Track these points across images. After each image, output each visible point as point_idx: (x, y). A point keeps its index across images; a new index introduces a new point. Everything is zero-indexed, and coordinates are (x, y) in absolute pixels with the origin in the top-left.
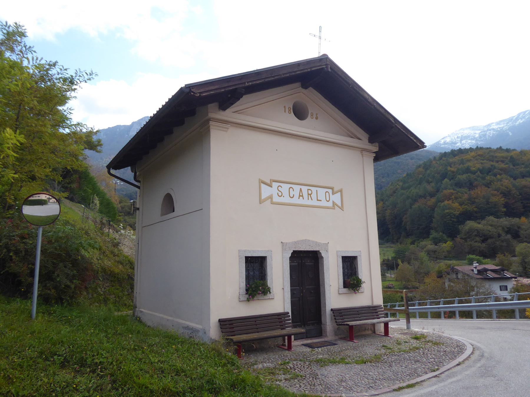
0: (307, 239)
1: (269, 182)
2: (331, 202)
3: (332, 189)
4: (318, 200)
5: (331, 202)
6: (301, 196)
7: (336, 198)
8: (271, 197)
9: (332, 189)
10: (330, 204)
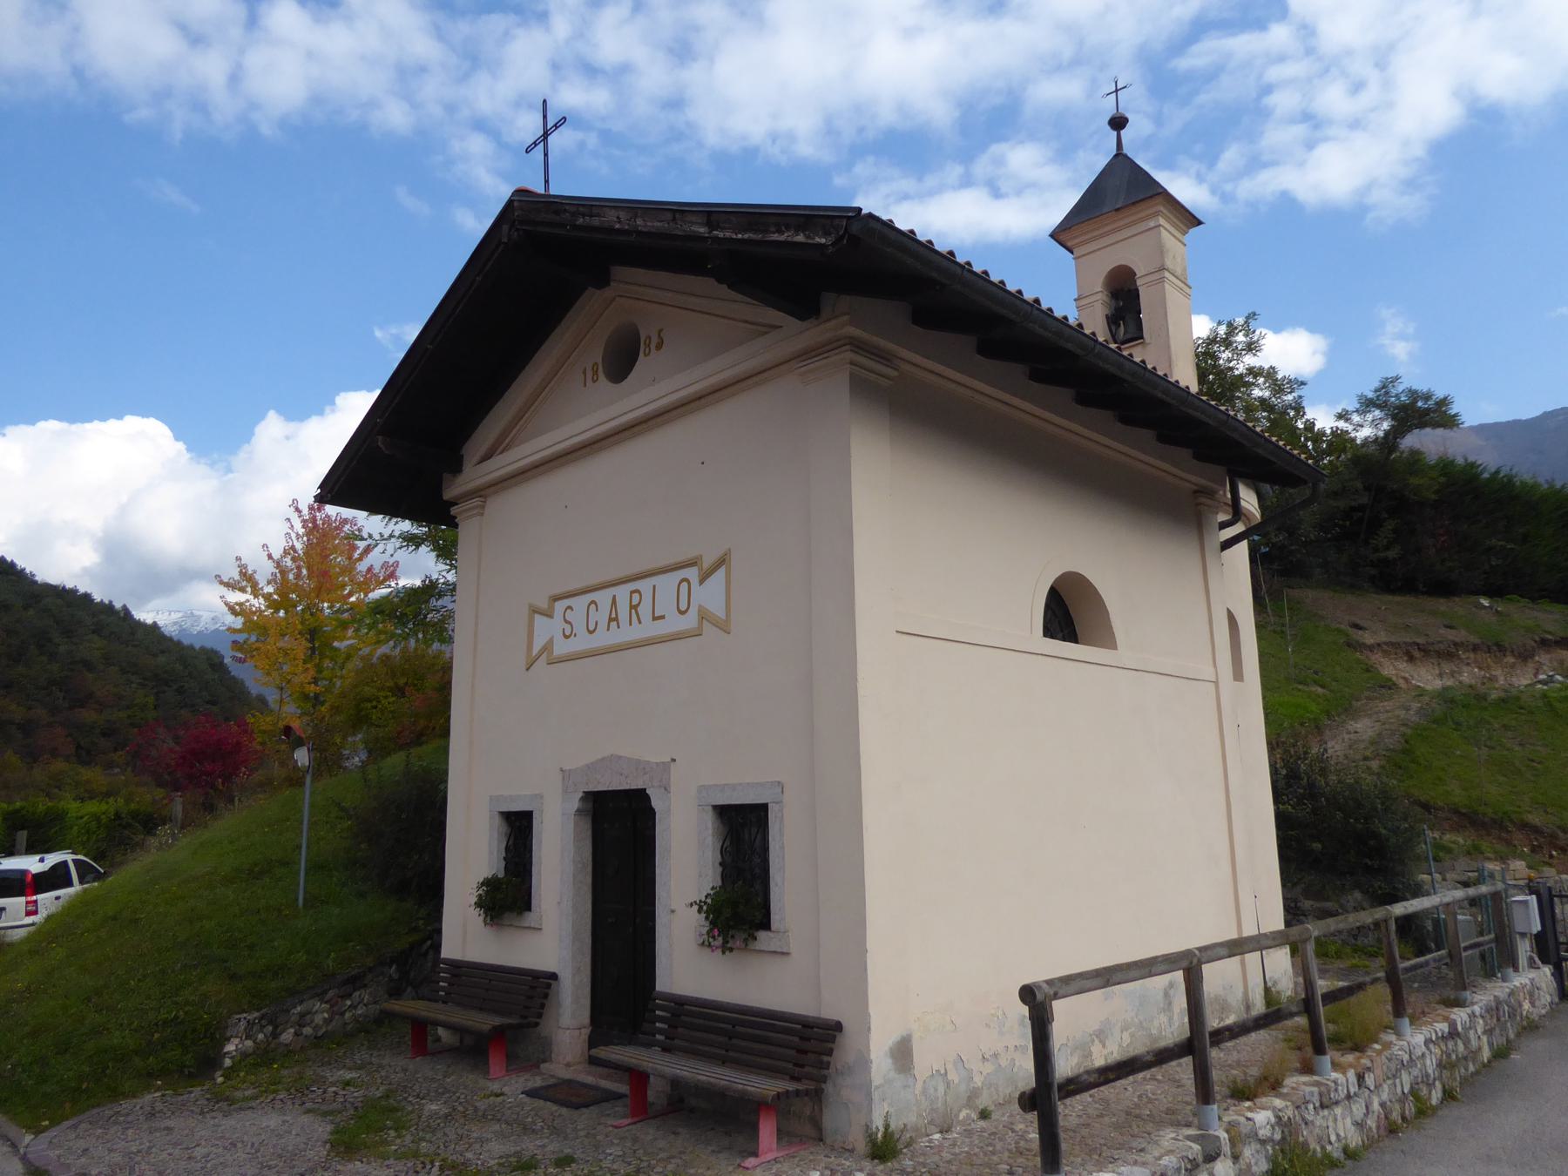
0: (618, 748)
1: (544, 604)
2: (693, 611)
3: (691, 563)
4: (655, 619)
5: (693, 611)
6: (613, 619)
7: (710, 595)
8: (548, 647)
9: (691, 563)
10: (689, 622)
